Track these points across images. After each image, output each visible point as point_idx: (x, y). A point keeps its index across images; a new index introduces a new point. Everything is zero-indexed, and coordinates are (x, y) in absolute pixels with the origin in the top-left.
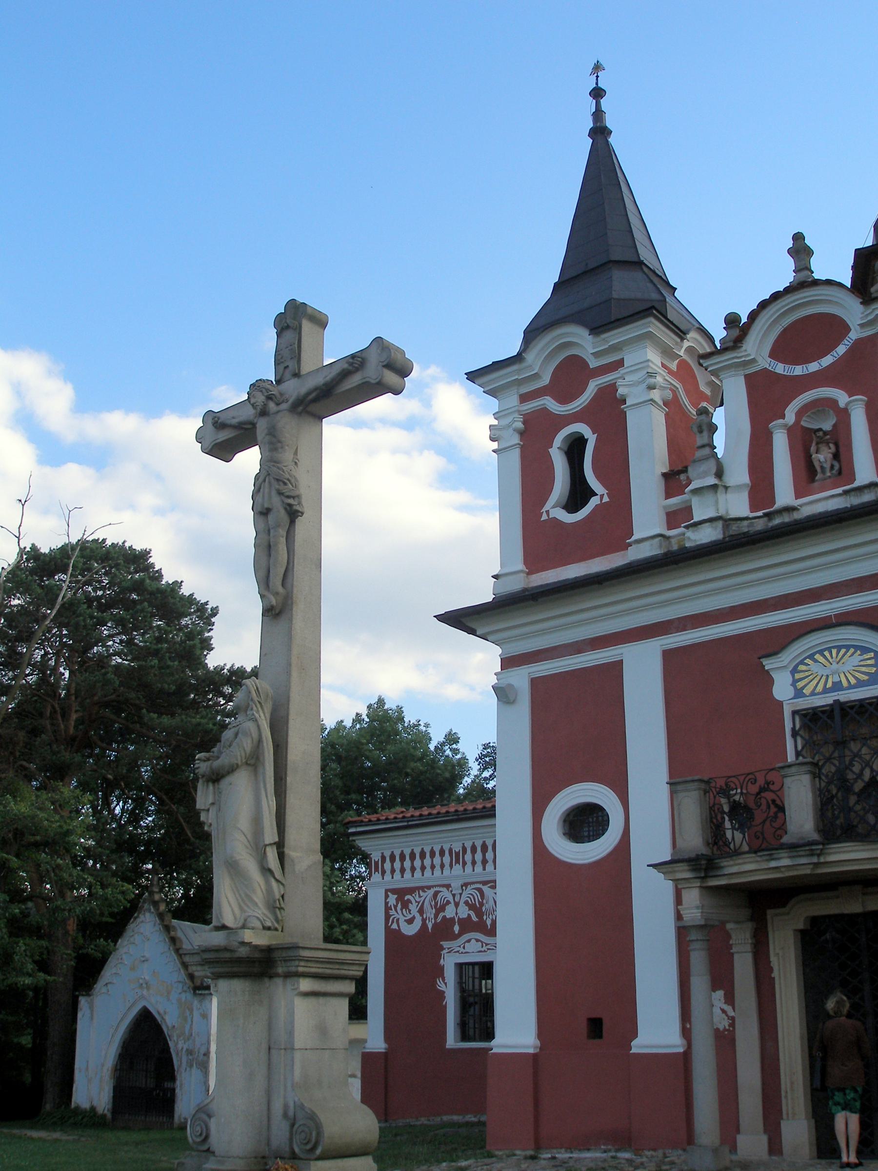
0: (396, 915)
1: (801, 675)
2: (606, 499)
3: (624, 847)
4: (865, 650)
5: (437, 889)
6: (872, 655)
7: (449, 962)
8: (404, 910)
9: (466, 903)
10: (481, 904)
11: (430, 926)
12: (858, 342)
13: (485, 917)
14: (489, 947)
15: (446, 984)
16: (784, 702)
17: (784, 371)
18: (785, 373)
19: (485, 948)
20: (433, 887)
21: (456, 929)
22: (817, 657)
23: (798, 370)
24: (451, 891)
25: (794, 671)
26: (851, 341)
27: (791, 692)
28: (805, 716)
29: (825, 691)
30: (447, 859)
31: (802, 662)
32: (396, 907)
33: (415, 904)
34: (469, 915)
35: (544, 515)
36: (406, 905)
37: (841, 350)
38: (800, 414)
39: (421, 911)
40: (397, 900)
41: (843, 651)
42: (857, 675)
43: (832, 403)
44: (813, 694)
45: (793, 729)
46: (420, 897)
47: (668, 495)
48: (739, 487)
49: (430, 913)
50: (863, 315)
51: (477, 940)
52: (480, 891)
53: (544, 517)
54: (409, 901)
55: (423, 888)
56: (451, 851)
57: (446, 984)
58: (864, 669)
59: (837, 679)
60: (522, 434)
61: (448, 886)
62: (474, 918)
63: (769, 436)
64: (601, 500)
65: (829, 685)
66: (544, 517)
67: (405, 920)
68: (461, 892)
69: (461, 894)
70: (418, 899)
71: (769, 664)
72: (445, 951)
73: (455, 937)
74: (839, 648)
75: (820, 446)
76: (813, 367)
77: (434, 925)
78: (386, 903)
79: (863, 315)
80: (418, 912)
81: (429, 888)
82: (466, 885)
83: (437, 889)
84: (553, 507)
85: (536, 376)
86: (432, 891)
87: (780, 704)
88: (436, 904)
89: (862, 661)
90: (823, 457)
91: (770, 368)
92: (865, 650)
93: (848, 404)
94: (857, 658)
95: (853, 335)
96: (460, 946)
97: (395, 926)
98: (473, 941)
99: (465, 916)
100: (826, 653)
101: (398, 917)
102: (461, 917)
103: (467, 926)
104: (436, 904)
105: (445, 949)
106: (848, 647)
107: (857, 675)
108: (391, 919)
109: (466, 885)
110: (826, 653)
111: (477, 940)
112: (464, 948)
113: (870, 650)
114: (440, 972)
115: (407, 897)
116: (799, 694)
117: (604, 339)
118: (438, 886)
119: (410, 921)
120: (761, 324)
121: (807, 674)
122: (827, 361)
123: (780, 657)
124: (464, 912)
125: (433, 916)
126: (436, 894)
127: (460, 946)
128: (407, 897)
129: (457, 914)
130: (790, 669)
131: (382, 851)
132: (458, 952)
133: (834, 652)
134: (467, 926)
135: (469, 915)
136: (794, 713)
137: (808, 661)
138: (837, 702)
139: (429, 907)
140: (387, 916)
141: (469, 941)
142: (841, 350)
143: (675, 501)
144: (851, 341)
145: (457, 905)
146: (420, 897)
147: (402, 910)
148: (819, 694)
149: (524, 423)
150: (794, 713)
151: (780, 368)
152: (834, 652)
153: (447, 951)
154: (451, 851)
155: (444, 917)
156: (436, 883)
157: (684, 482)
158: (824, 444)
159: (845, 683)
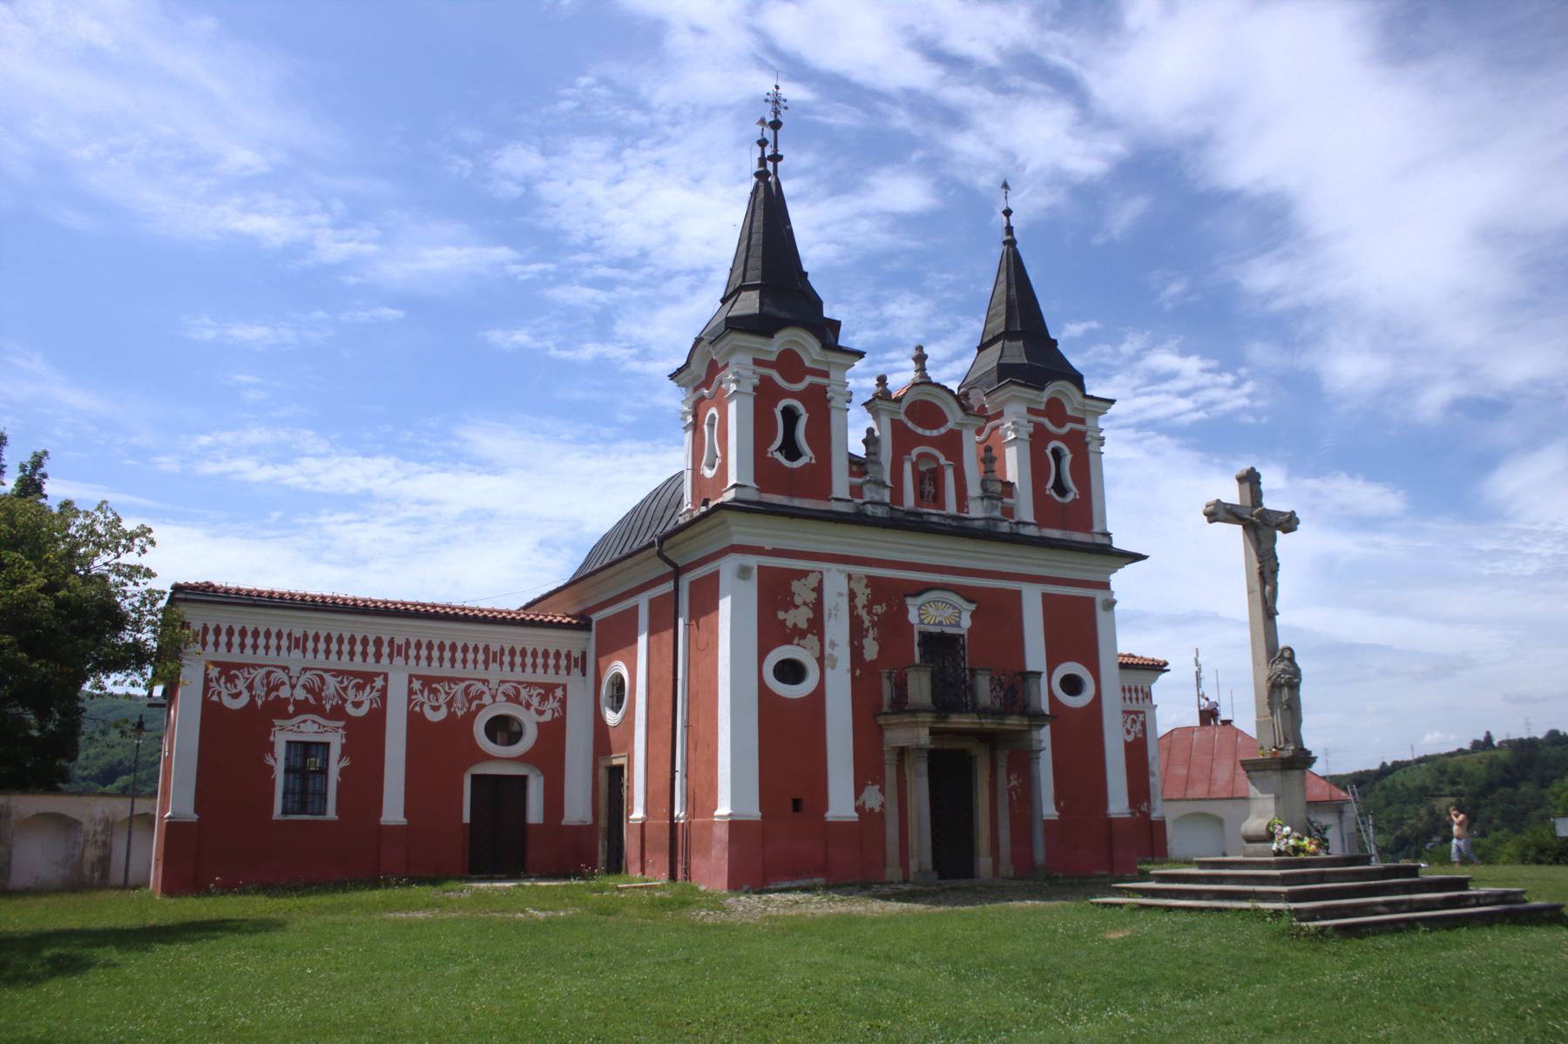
0: (218, 688)
4: (954, 608)
5: (271, 669)
7: (280, 740)
8: (228, 685)
9: (304, 686)
10: (321, 690)
11: (260, 703)
12: (951, 431)
13: (324, 702)
14: (325, 729)
15: (275, 759)
19: (322, 730)
20: (266, 666)
21: (291, 709)
23: (919, 431)
24: (288, 673)
25: (920, 608)
29: (935, 624)
30: (284, 643)
31: (923, 605)
32: (218, 680)
33: (242, 680)
34: (307, 698)
36: (231, 679)
37: (943, 430)
38: (920, 456)
39: (250, 687)
40: (221, 674)
41: (944, 605)
43: (936, 459)
44: (929, 624)
46: (249, 673)
49: (260, 691)
51: (314, 722)
52: (322, 678)
53: (769, 455)
54: (236, 676)
55: (254, 666)
56: (289, 636)
57: (275, 759)
60: (755, 388)
61: (285, 668)
62: (312, 700)
65: (937, 622)
66: (769, 455)
67: (229, 694)
68: (298, 675)
69: (298, 678)
70: (246, 675)
71: (909, 601)
72: (275, 729)
73: (290, 717)
76: (928, 433)
77: (264, 703)
78: (206, 675)
80: (246, 687)
81: (262, 666)
82: (305, 670)
83: (271, 669)
84: (776, 451)
85: (772, 352)
86: (263, 671)
87: (912, 626)
88: (268, 683)
90: (929, 489)
92: (954, 608)
94: (950, 611)
95: (950, 425)
96: (294, 726)
97: (215, 698)
98: (309, 722)
99: (302, 698)
101: (220, 689)
102: (298, 698)
103: (302, 707)
104: (268, 683)
105: (276, 726)
106: (947, 603)
108: (211, 690)
109: (305, 670)
111: (314, 722)
112: (298, 727)
114: (270, 747)
115: (232, 672)
116: (921, 622)
118: (275, 666)
119: (236, 696)
122: (935, 433)
124: (300, 694)
125: (263, 694)
126: (269, 674)
127: (294, 726)
128: (232, 672)
129: (292, 695)
131: (243, 625)
132: (291, 730)
133: (940, 604)
134: (302, 707)
135: (307, 698)
139: (260, 686)
140: (206, 688)
141: (304, 721)
142: (943, 430)
145: (293, 687)
146: (249, 673)
147: (225, 683)
149: (760, 380)
150: (920, 632)
151: (910, 424)
153: (278, 728)
154: (289, 636)
155: (277, 697)
156: (269, 663)
159: (944, 623)
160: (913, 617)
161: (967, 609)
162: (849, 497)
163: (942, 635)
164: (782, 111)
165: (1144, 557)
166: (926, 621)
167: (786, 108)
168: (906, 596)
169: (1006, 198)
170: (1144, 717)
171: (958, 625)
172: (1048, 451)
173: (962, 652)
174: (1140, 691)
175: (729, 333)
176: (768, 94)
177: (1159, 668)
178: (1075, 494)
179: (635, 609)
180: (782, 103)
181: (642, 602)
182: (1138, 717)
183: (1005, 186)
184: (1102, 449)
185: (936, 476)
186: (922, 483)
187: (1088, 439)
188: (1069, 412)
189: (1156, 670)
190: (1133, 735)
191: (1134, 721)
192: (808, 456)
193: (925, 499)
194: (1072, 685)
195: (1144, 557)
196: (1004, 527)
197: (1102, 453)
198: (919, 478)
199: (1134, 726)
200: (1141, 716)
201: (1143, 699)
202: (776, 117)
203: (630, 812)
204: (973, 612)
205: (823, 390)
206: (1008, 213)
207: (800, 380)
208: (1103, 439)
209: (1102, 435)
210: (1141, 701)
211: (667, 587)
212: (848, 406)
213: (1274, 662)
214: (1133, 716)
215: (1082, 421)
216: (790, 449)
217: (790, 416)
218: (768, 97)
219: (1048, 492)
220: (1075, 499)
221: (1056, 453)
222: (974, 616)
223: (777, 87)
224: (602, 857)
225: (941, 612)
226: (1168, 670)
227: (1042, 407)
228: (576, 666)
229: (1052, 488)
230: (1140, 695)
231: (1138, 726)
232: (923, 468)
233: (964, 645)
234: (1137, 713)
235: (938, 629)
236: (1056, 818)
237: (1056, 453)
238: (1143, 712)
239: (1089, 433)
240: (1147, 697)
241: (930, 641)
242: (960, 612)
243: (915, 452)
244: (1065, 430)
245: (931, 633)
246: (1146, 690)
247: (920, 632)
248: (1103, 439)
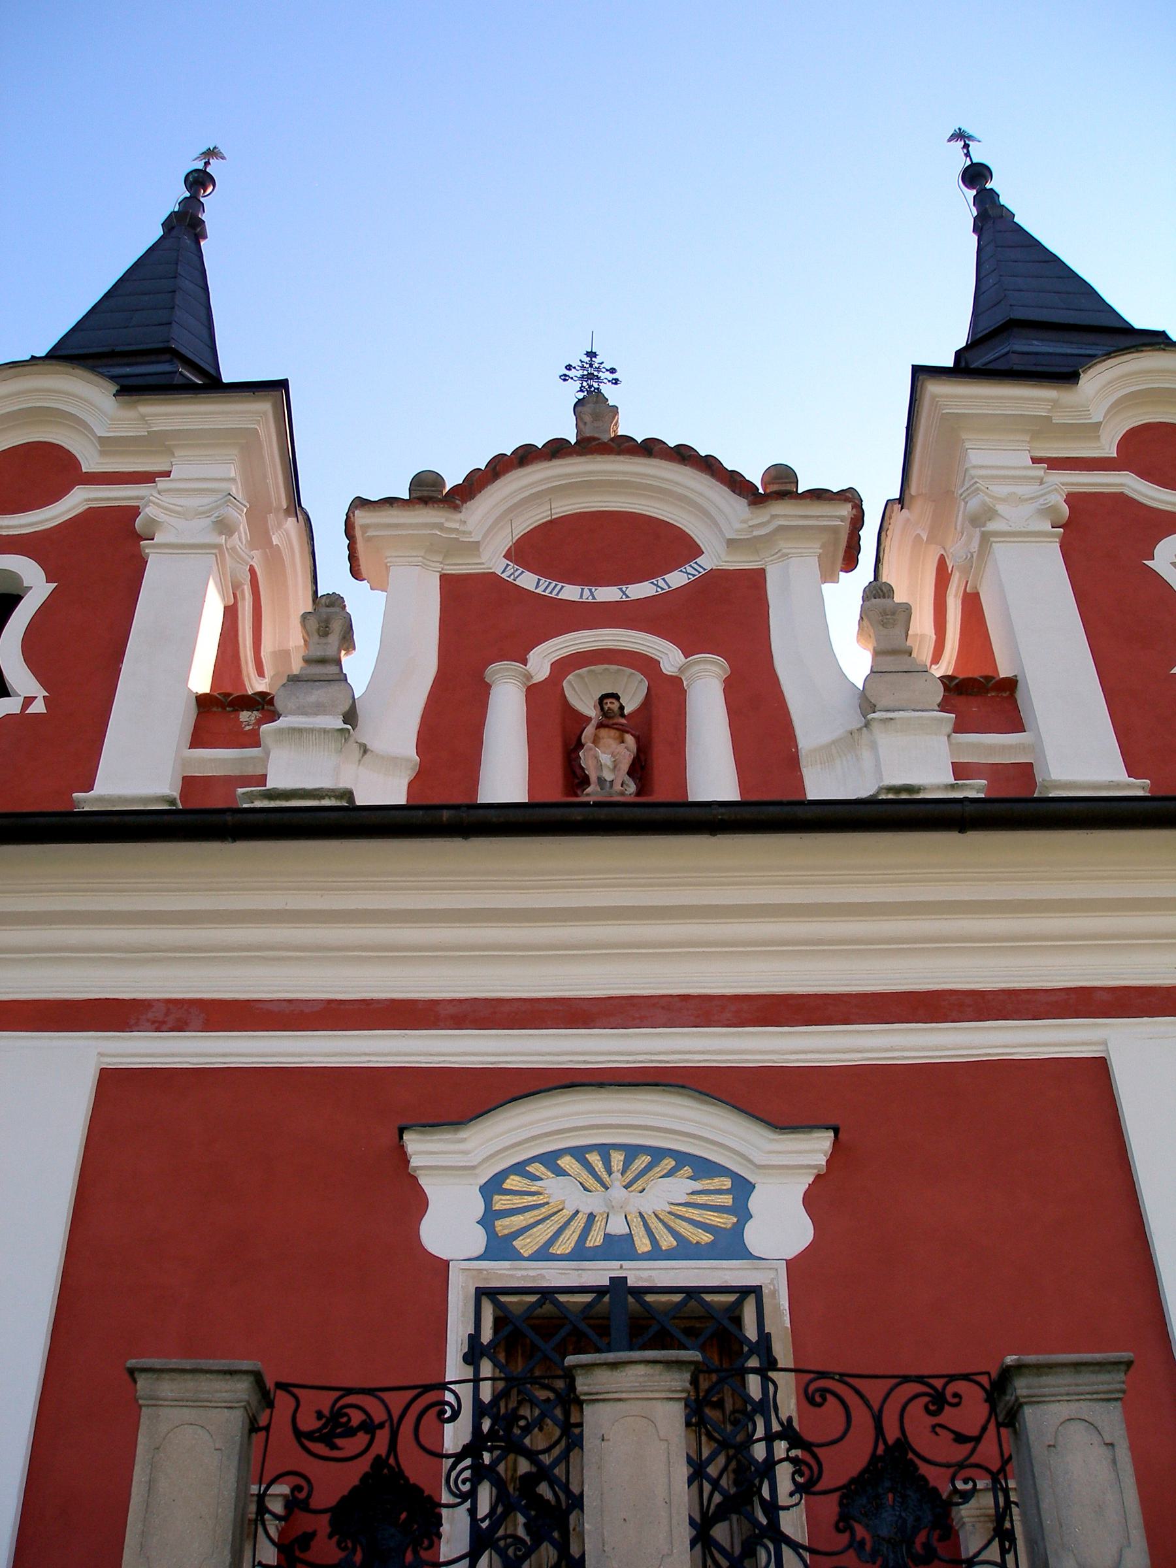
2: (38, 707)
6: (727, 1183)
12: (715, 578)
17: (537, 587)
18: (539, 591)
22: (566, 1162)
23: (571, 592)
26: (701, 570)
27: (478, 1241)
29: (580, 1253)
31: (519, 1169)
37: (676, 579)
41: (643, 1160)
43: (646, 665)
44: (543, 1254)
45: (474, 1339)
47: (197, 741)
48: (394, 762)
50: (745, 526)
59: (617, 1227)
63: (481, 694)
65: (595, 1239)
74: (632, 1151)
75: (604, 732)
76: (608, 594)
79: (745, 526)
87: (442, 1267)
89: (693, 1193)
92: (703, 1168)
93: (681, 669)
94: (680, 1187)
100: (594, 1158)
106: (658, 1154)
107: (685, 1229)
110: (594, 1158)
113: (722, 1171)
117: (143, 417)
120: (515, 486)
122: (641, 590)
123: (463, 1141)
130: (483, 1181)
133: (617, 1158)
136: (482, 1293)
137: (536, 1168)
138: (619, 1283)
142: (676, 579)
144: (701, 570)
150: (482, 1293)
151: (528, 581)
152: (617, 1158)
157: (248, 728)
158: (613, 733)
159: (643, 1244)
166: (524, 1243)
176: (569, 367)
218: (571, 373)
225: (617, 1192)
233: (765, 1339)
235: (598, 1274)
242: (743, 1188)
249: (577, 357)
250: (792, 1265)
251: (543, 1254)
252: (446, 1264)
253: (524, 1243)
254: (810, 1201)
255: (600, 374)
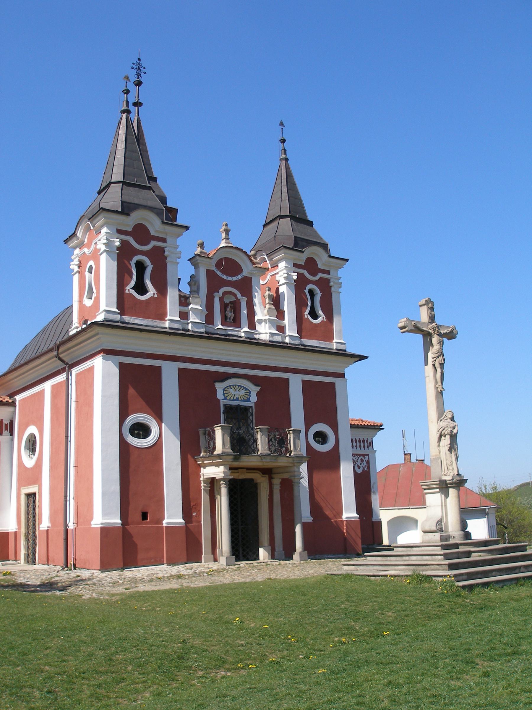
1: (227, 392)
3: (158, 443)
16: (221, 401)
22: (232, 387)
23: (225, 277)
25: (224, 390)
28: (228, 407)
29: (233, 400)
31: (226, 387)
35: (127, 290)
37: (240, 277)
38: (225, 293)
41: (240, 387)
42: (244, 397)
43: (235, 296)
45: (224, 411)
58: (246, 396)
59: (238, 397)
64: (154, 295)
65: (235, 398)
66: (127, 291)
74: (239, 386)
76: (230, 278)
84: (131, 289)
90: (230, 314)
91: (215, 271)
92: (246, 389)
94: (243, 392)
100: (235, 386)
106: (241, 387)
107: (244, 397)
110: (235, 386)
113: (249, 390)
116: (225, 398)
121: (228, 392)
122: (235, 279)
137: (228, 387)
142: (240, 277)
143: (183, 309)
148: (231, 400)
150: (224, 405)
151: (218, 273)
159: (240, 399)
160: (220, 395)
161: (254, 390)
162: (179, 319)
163: (238, 407)
164: (142, 74)
165: (367, 357)
166: (228, 398)
167: (145, 73)
168: (215, 382)
169: (282, 132)
170: (369, 458)
171: (248, 400)
172: (306, 291)
173: (251, 418)
174: (366, 442)
175: (101, 212)
176: (134, 64)
177: (378, 428)
178: (323, 318)
179: (42, 392)
180: (142, 69)
181: (47, 386)
182: (365, 458)
183: (282, 124)
184: (340, 290)
185: (235, 306)
186: (226, 310)
187: (331, 284)
188: (320, 266)
189: (376, 429)
190: (361, 468)
191: (362, 461)
192: (152, 292)
193: (228, 320)
194: (321, 437)
195: (367, 358)
196: (278, 339)
197: (341, 292)
198: (224, 307)
199: (362, 464)
200: (367, 457)
201: (368, 447)
202: (138, 78)
203: (40, 522)
204: (258, 392)
205: (162, 250)
206: (283, 141)
207: (147, 243)
208: (341, 283)
209: (340, 281)
210: (366, 448)
211: (61, 378)
212: (178, 260)
213: (442, 420)
214: (362, 457)
215: (328, 272)
216: (141, 288)
217: (141, 267)
219: (306, 317)
220: (323, 321)
221: (311, 292)
222: (258, 394)
223: (139, 60)
224: (23, 552)
226: (383, 429)
227: (303, 263)
228: (6, 429)
229: (308, 314)
230: (366, 444)
231: (365, 462)
232: (227, 301)
234: (364, 455)
235: (236, 403)
236: (311, 521)
237: (311, 292)
238: (368, 455)
239: (331, 280)
240: (370, 446)
241: (229, 409)
242: (250, 392)
243: (222, 290)
244: (316, 278)
245: (231, 405)
246: (370, 441)
247: (224, 405)
248: (341, 283)
249: (135, 60)
250: (255, 403)
251: (230, 400)
252: (220, 400)
253: (228, 398)
254: (257, 395)
255: (141, 69)
